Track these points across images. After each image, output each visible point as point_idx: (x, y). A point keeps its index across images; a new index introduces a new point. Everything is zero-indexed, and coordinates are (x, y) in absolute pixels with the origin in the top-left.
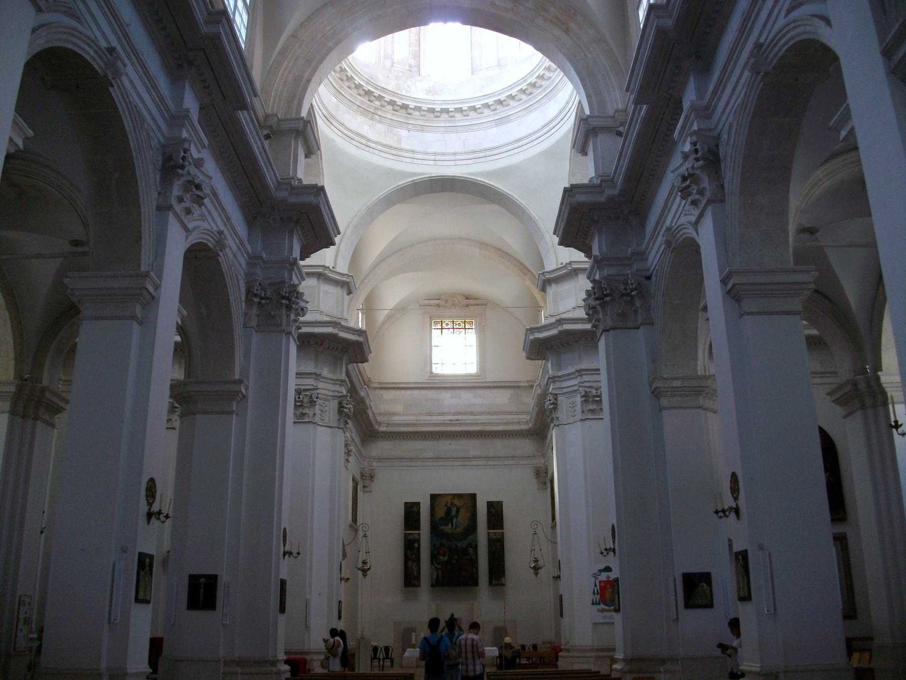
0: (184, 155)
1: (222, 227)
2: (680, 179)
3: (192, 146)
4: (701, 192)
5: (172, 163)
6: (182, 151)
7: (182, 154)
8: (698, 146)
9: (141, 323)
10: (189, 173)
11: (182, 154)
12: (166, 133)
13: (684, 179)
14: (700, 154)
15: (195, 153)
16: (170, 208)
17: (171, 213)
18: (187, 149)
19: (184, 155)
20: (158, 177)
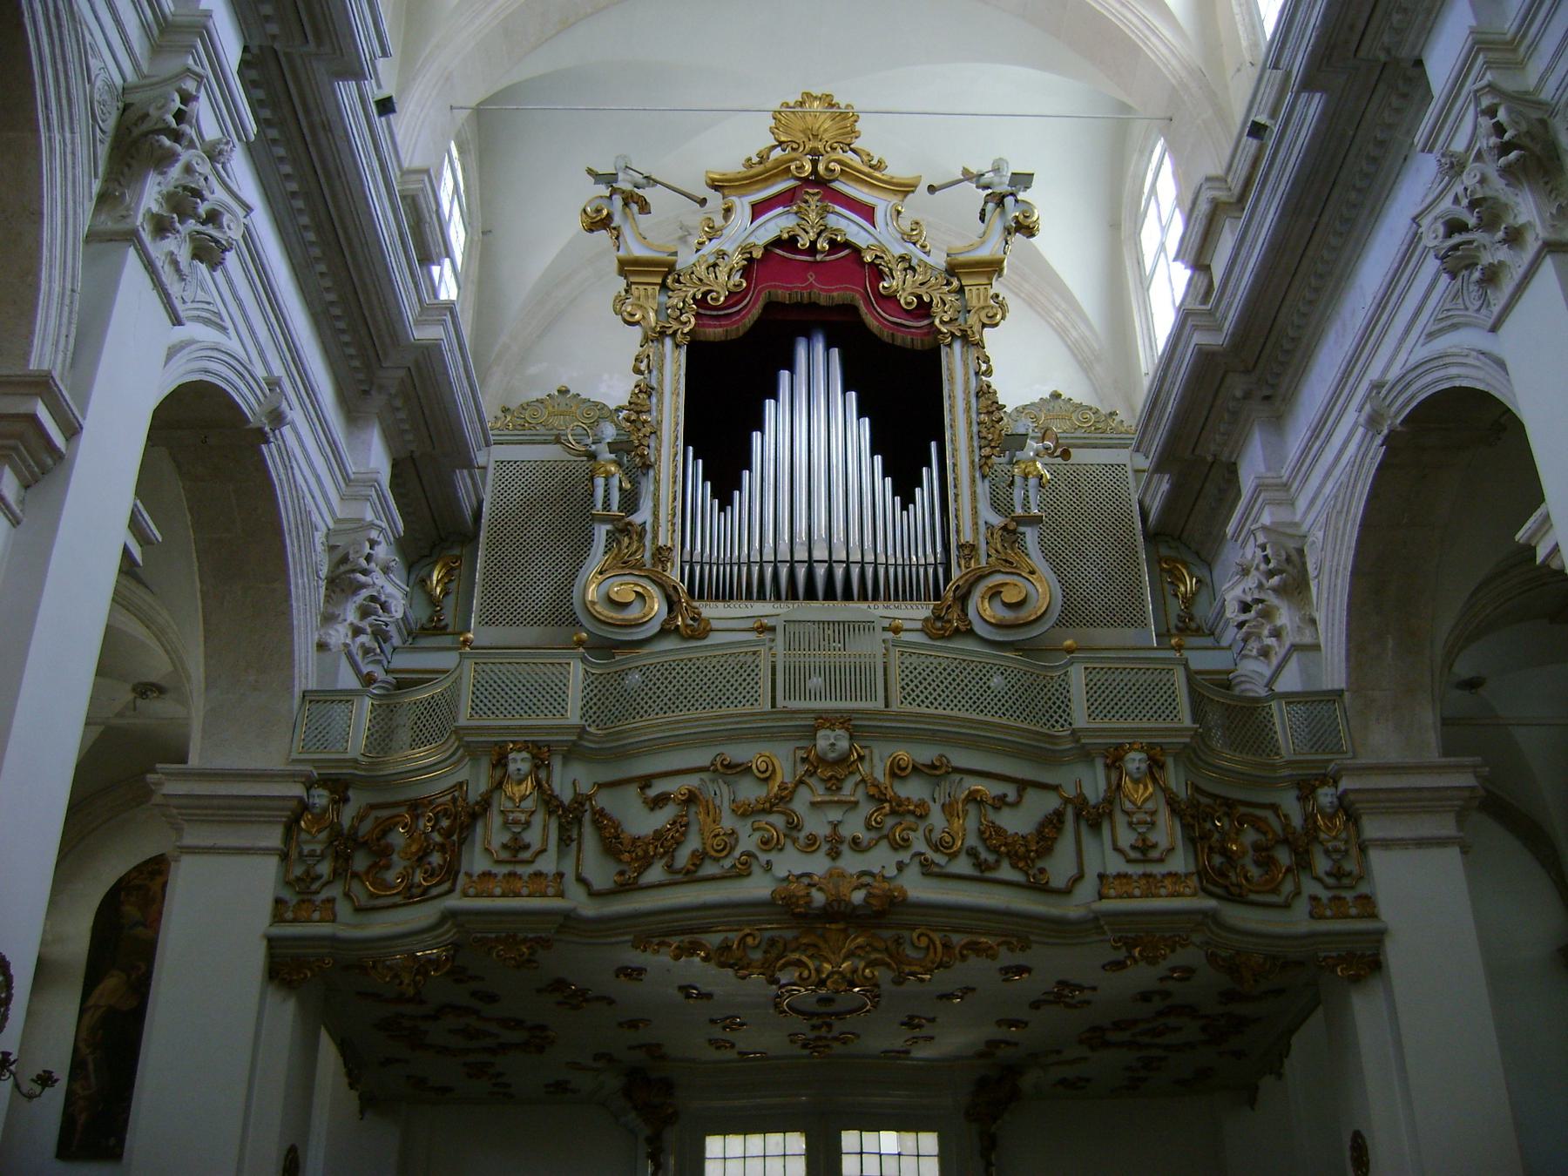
0: (183, 107)
1: (278, 370)
2: (1441, 230)
3: (203, 95)
4: (1514, 237)
5: (145, 127)
6: (177, 98)
7: (177, 104)
8: (1502, 115)
9: (15, 521)
10: (189, 169)
11: (177, 104)
12: (145, 68)
13: (1454, 226)
14: (1507, 137)
15: (208, 122)
16: (132, 237)
17: (132, 252)
18: (191, 94)
19: (183, 107)
20: (103, 151)
